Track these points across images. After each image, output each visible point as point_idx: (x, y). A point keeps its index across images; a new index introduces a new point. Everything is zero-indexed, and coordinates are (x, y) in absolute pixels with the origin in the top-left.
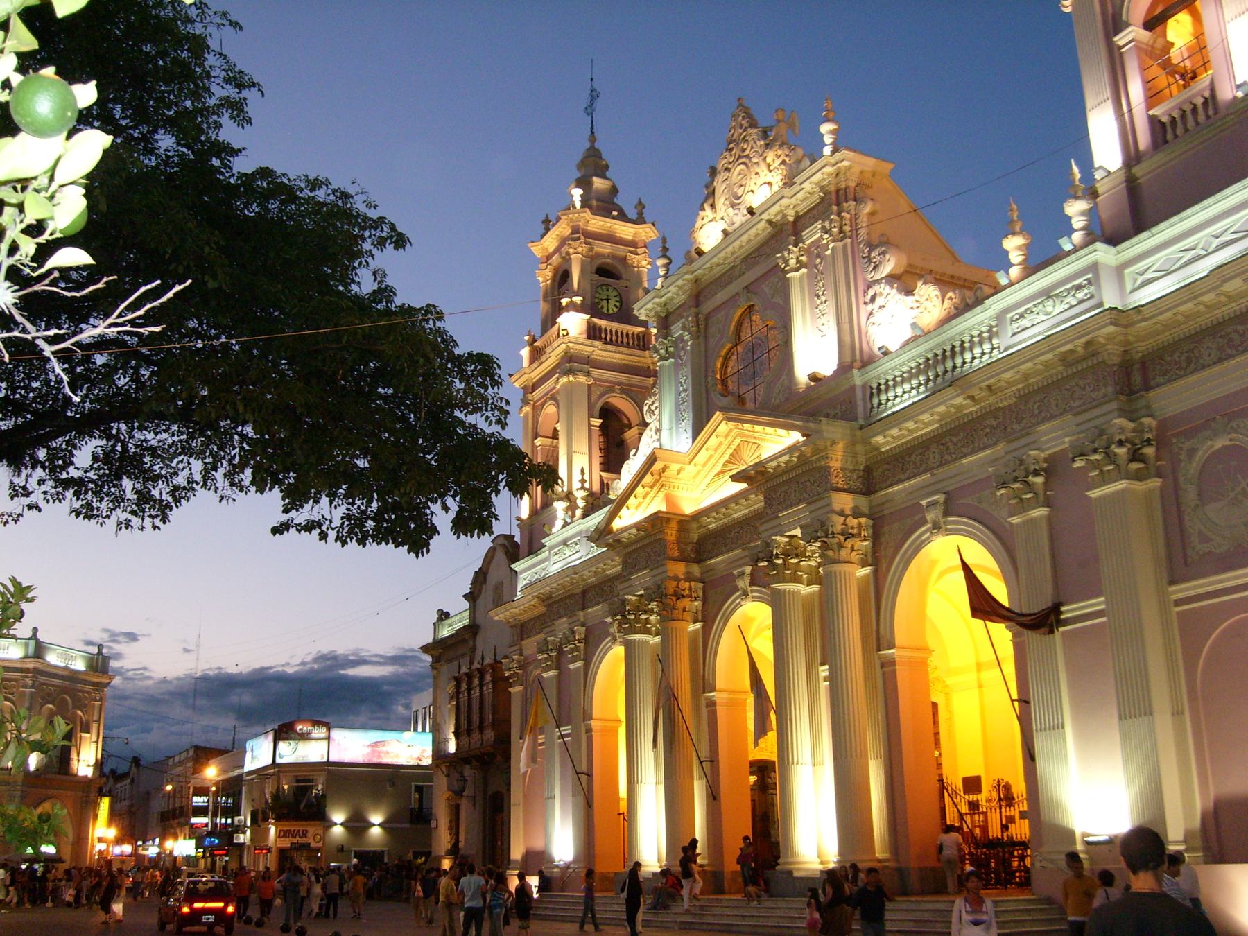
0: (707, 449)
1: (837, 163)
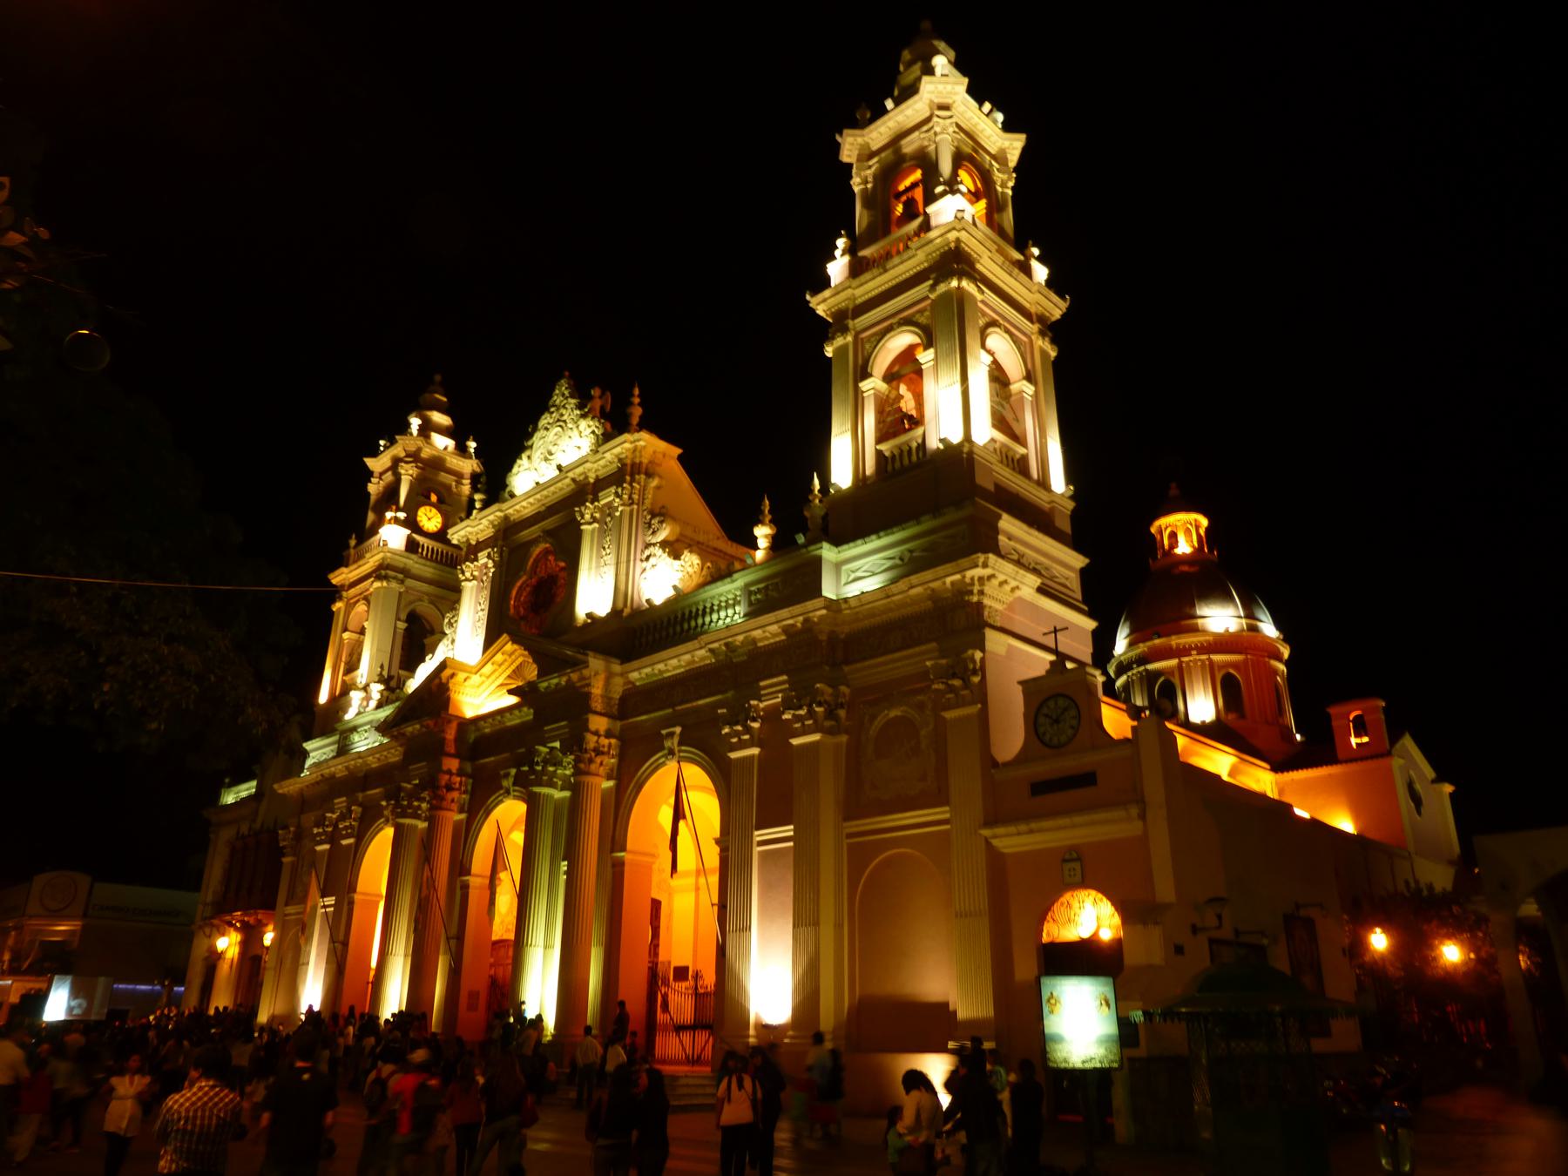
1: (635, 441)
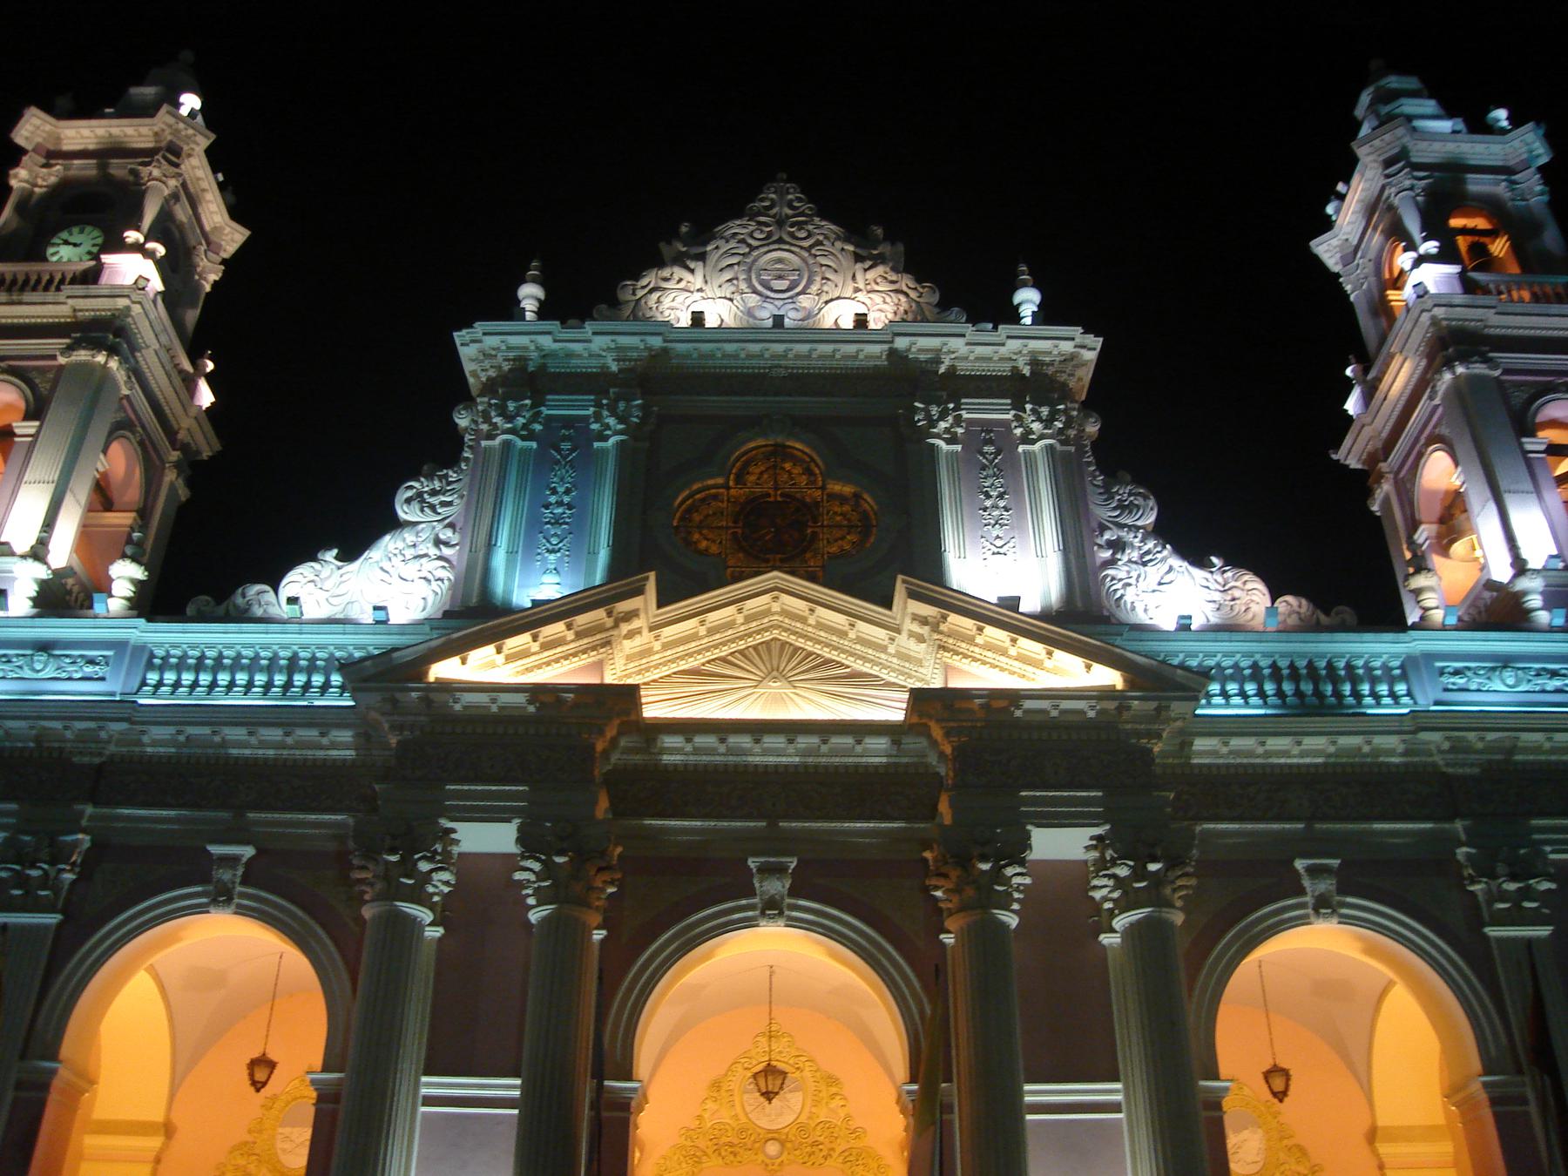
0: (702, 623)
